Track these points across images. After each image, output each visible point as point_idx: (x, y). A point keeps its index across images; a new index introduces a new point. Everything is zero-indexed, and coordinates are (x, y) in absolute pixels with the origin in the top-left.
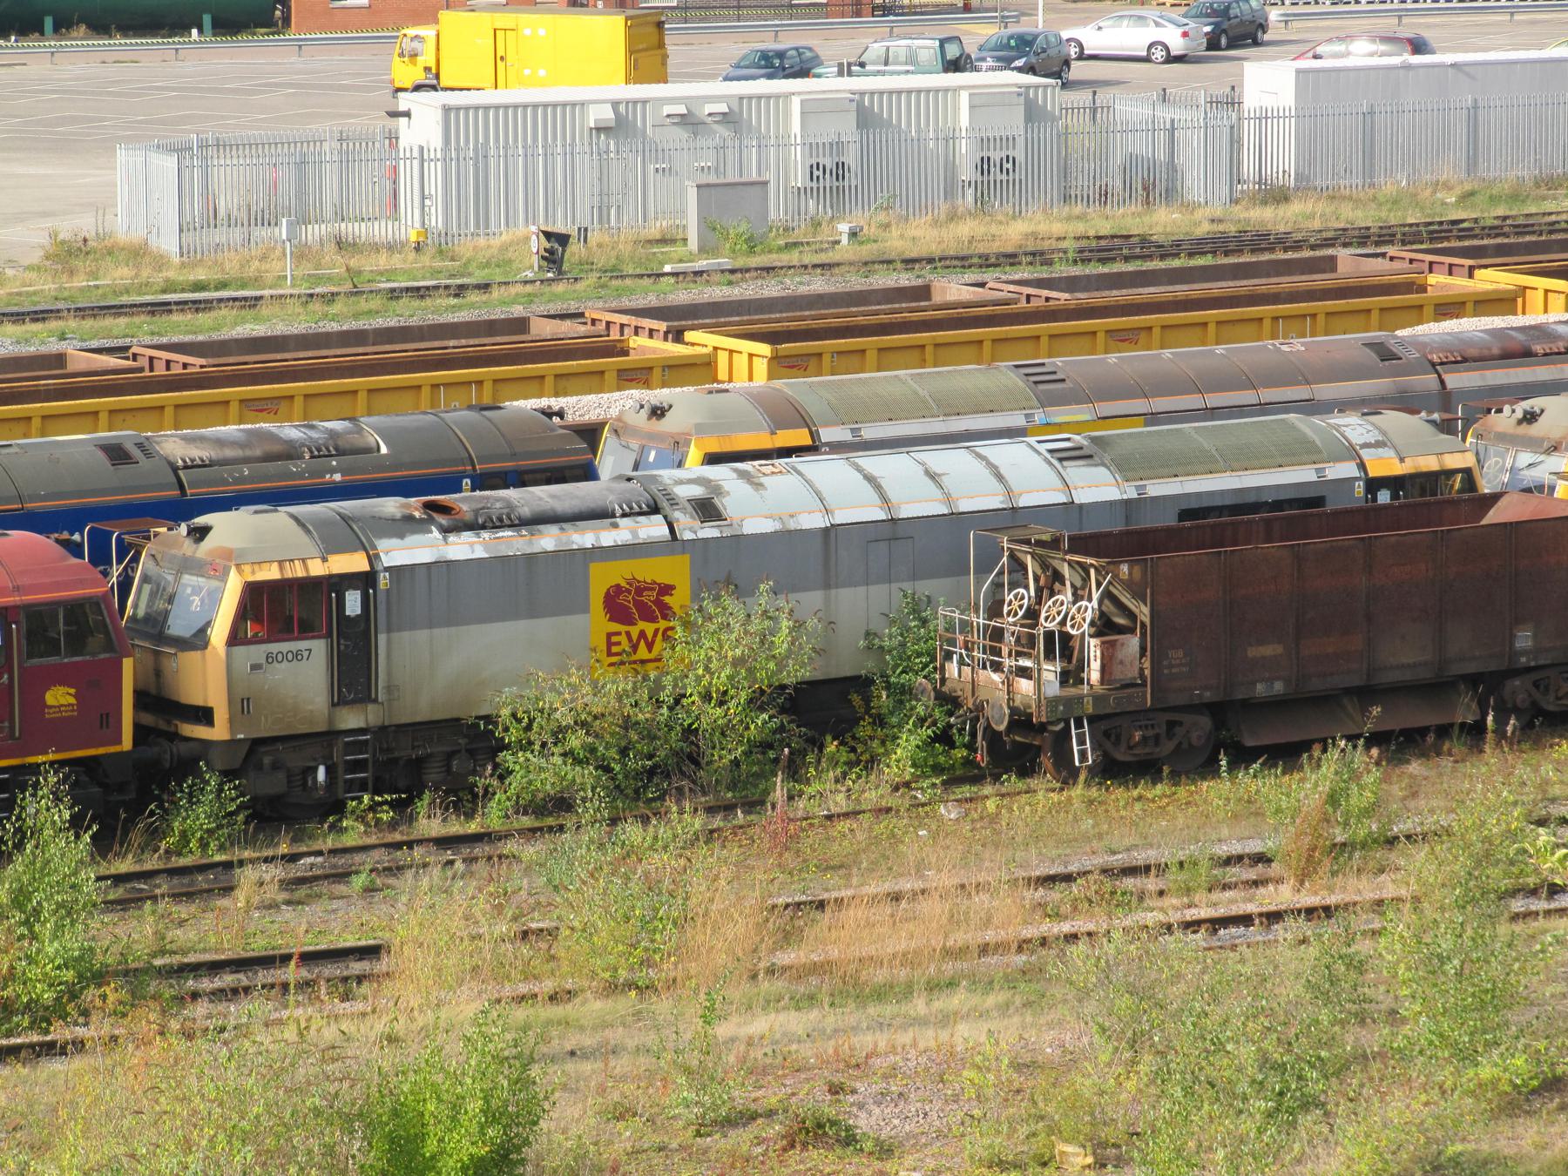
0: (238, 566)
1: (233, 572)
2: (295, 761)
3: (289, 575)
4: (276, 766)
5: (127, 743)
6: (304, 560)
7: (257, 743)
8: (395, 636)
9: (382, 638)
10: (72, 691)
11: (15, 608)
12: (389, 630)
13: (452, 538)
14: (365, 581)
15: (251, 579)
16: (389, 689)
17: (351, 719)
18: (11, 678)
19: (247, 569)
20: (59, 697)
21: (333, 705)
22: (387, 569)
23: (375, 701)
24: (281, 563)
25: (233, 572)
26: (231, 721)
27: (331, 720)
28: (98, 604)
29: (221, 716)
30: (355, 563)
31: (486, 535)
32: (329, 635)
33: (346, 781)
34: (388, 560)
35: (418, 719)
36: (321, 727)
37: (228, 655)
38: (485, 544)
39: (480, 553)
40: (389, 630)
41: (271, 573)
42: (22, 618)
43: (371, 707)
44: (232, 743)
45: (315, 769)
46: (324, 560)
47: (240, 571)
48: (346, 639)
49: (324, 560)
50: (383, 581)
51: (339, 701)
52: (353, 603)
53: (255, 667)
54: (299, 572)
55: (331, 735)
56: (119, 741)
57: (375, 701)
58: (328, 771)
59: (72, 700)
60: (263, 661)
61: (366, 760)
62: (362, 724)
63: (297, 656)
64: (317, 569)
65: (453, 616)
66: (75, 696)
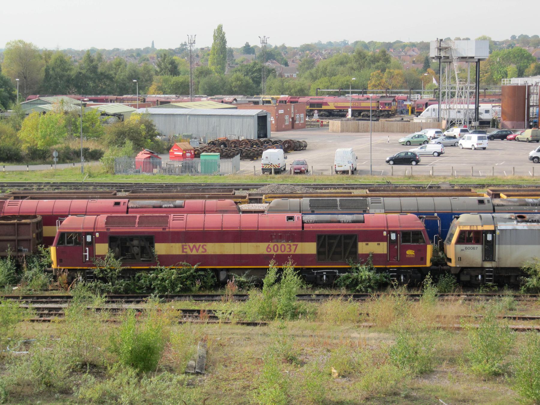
0: (459, 226)
1: (458, 227)
2: (473, 273)
3: (472, 229)
4: (467, 274)
5: (428, 264)
6: (477, 226)
7: (463, 269)
8: (501, 246)
9: (497, 246)
10: (414, 251)
11: (399, 231)
12: (499, 244)
13: (519, 224)
14: (493, 232)
15: (462, 229)
16: (499, 259)
17: (488, 265)
18: (398, 247)
19: (461, 227)
20: (410, 253)
21: (483, 261)
22: (499, 230)
23: (495, 261)
24: (471, 226)
25: (458, 227)
26: (456, 262)
27: (482, 264)
28: (421, 232)
29: (453, 260)
30: (491, 228)
31: (528, 224)
32: (482, 244)
33: (487, 279)
34: (499, 228)
35: (507, 266)
36: (480, 266)
37: (455, 247)
38: (528, 226)
39: (526, 228)
40: (499, 244)
41: (468, 228)
42: (401, 233)
43: (493, 262)
44: (456, 268)
45: (478, 276)
46: (482, 226)
47: (459, 227)
48: (487, 245)
49: (482, 226)
50: (498, 232)
51: (484, 260)
52: (489, 237)
53: (462, 250)
54: (475, 229)
55: (482, 268)
56: (426, 264)
57: (495, 261)
58: (482, 276)
59: (414, 254)
60: (464, 249)
61: (492, 275)
62: (491, 266)
63: (473, 248)
64: (480, 228)
65: (517, 243)
66: (415, 253)
